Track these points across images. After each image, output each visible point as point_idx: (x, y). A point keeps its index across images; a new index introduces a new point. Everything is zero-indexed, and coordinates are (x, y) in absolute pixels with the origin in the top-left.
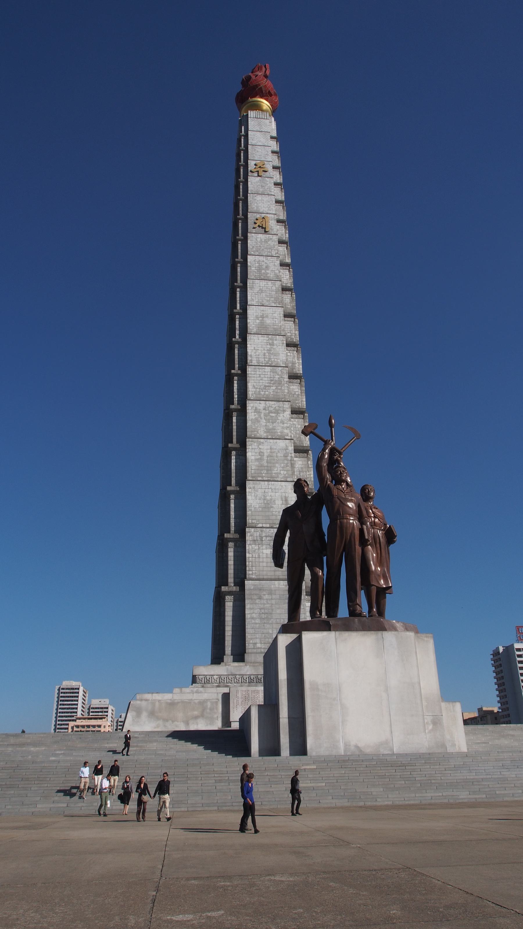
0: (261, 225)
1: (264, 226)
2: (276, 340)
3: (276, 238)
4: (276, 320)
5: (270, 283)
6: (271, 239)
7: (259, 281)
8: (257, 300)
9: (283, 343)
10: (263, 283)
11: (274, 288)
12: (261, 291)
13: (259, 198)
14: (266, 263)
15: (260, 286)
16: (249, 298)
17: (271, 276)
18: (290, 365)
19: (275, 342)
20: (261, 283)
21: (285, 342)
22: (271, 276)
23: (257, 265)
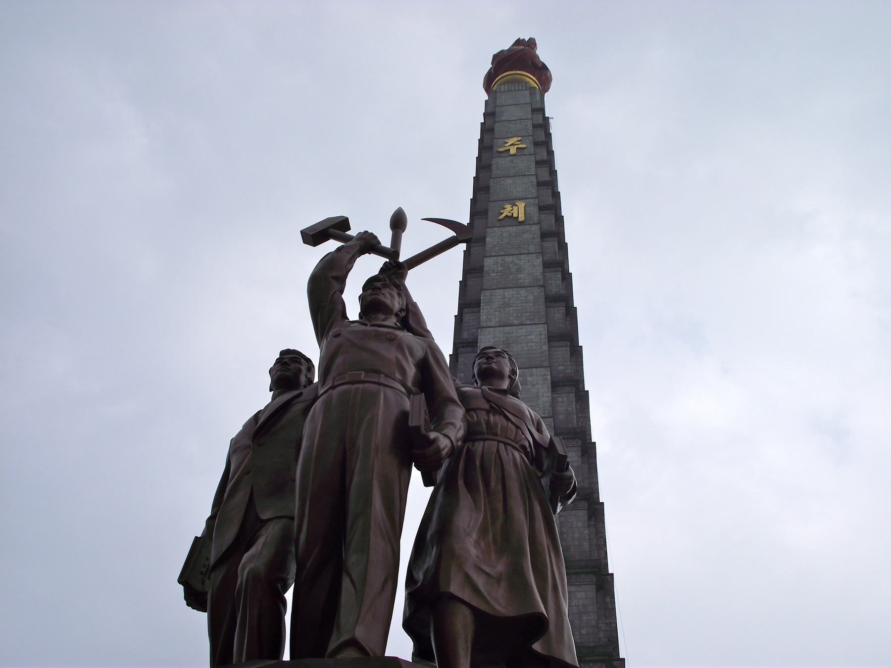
0: (509, 214)
1: (515, 215)
2: (531, 375)
3: (536, 229)
4: (533, 344)
5: (523, 292)
6: (527, 231)
7: (501, 291)
8: (497, 320)
9: (546, 379)
10: (509, 293)
11: (531, 297)
12: (506, 305)
13: (509, 181)
14: (516, 264)
15: (504, 298)
16: (483, 317)
17: (527, 281)
18: (562, 417)
19: (529, 379)
20: (507, 293)
21: (549, 377)
22: (524, 278)
23: (500, 269)
